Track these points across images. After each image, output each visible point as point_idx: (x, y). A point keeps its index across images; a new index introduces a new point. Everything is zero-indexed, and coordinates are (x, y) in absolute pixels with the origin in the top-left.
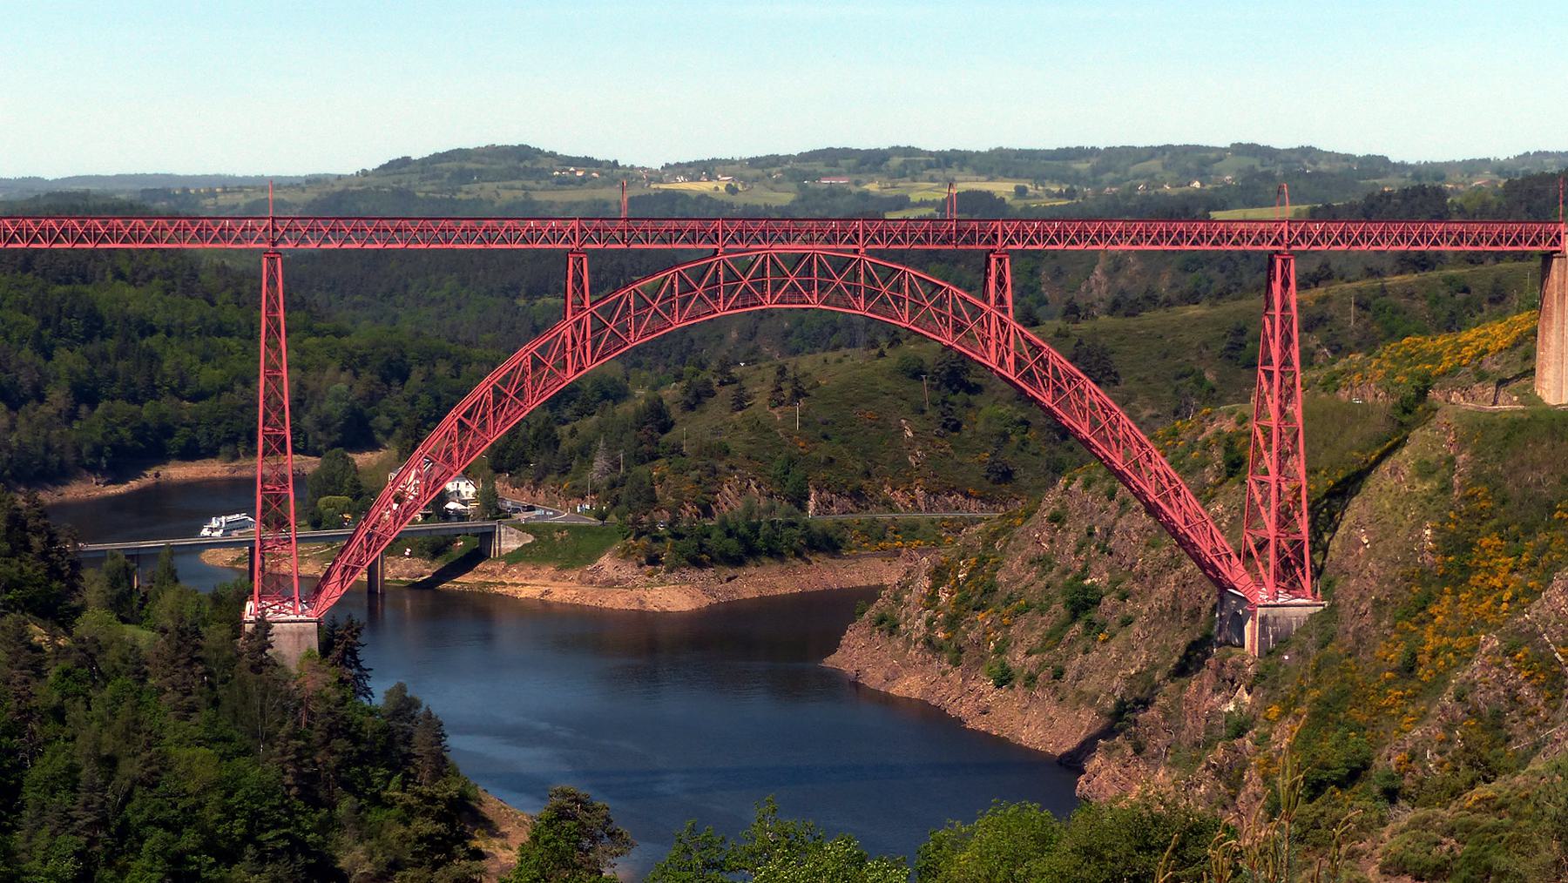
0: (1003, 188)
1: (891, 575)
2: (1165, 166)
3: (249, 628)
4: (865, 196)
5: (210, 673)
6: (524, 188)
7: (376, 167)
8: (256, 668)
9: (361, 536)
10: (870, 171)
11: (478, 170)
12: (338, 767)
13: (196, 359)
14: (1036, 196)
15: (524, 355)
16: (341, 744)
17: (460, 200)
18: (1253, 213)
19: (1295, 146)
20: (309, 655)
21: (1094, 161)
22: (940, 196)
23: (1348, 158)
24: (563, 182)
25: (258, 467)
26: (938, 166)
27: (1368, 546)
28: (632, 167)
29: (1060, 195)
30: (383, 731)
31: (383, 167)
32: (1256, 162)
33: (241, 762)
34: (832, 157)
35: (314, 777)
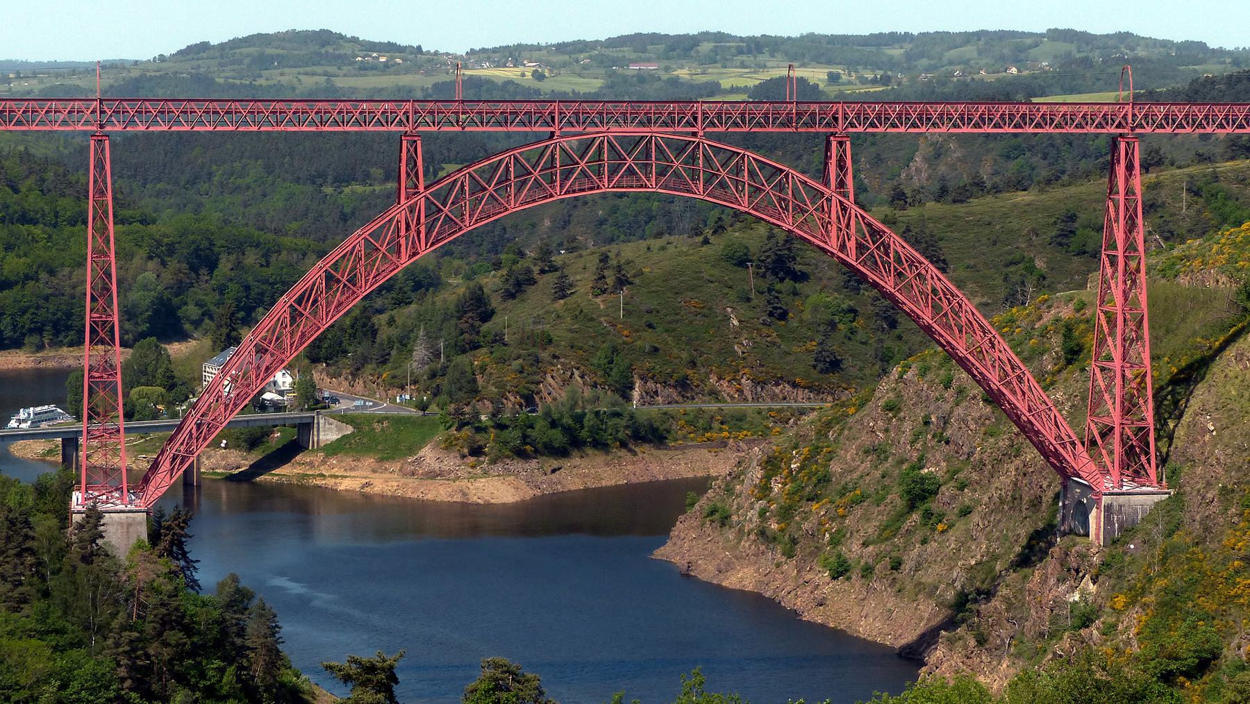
0: (816, 75)
1: (719, 465)
2: (980, 53)
3: (77, 518)
4: (675, 82)
5: (40, 564)
6: (326, 74)
7: (174, 52)
8: (87, 559)
9: (191, 425)
10: (679, 57)
11: (278, 55)
12: (171, 660)
14: (850, 83)
15: (358, 238)
16: (174, 636)
17: (261, 85)
18: (1070, 99)
19: (1112, 32)
20: (140, 546)
21: (908, 46)
22: (751, 83)
23: (1165, 44)
24: (364, 69)
25: (85, 357)
26: (749, 52)
27: (1214, 433)
28: (436, 53)
29: (874, 82)
30: (221, 622)
31: (181, 52)
32: (1072, 48)
33: (75, 653)
34: (640, 43)
35: (148, 670)
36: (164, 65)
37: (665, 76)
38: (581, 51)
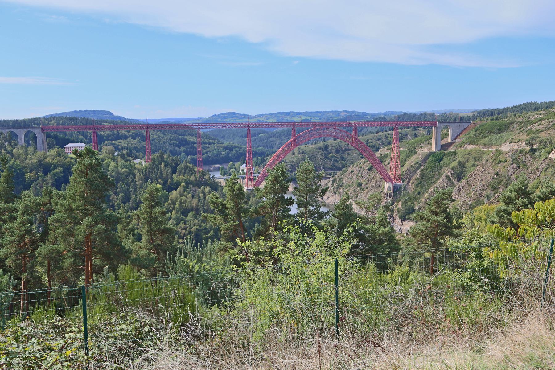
0: (309, 118)
4: (287, 120)
23: (360, 113)
24: (240, 118)
34: (281, 113)
37: (286, 119)
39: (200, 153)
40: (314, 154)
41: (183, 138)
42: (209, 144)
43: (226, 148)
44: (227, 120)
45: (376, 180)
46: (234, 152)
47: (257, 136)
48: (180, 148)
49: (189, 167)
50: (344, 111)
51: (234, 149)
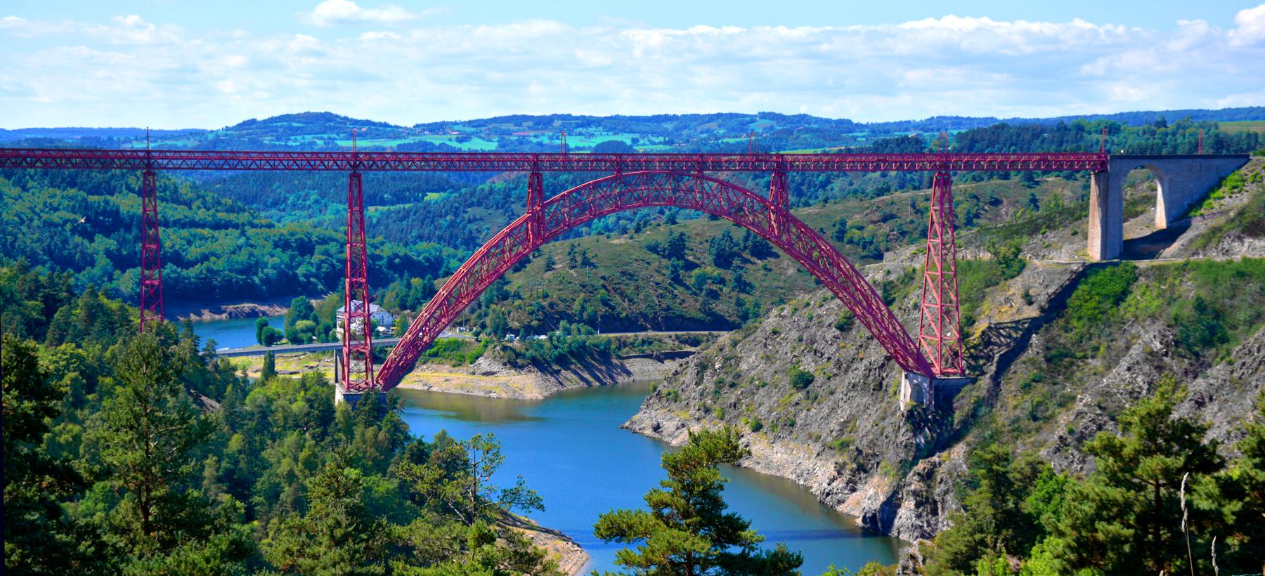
0: (626, 139)
4: (540, 144)
13: (184, 242)
22: (593, 145)
23: (828, 121)
24: (353, 136)
28: (397, 127)
31: (239, 125)
34: (518, 120)
36: (229, 132)
37: (535, 140)
38: (483, 126)
39: (178, 259)
40: (630, 269)
41: (107, 203)
42: (217, 226)
43: (283, 244)
44: (295, 143)
45: (865, 362)
46: (317, 258)
47: (417, 200)
48: (92, 240)
49: (107, 313)
50: (764, 116)
51: (319, 249)
